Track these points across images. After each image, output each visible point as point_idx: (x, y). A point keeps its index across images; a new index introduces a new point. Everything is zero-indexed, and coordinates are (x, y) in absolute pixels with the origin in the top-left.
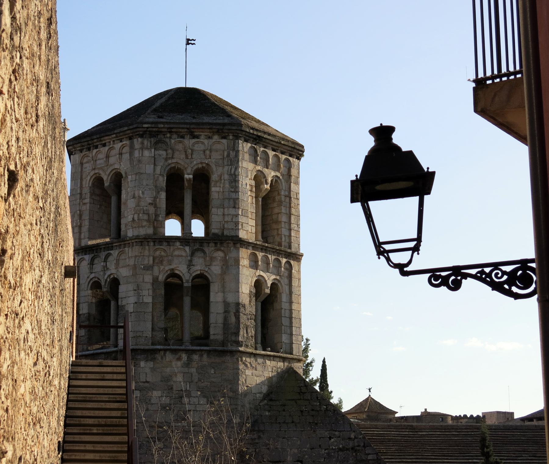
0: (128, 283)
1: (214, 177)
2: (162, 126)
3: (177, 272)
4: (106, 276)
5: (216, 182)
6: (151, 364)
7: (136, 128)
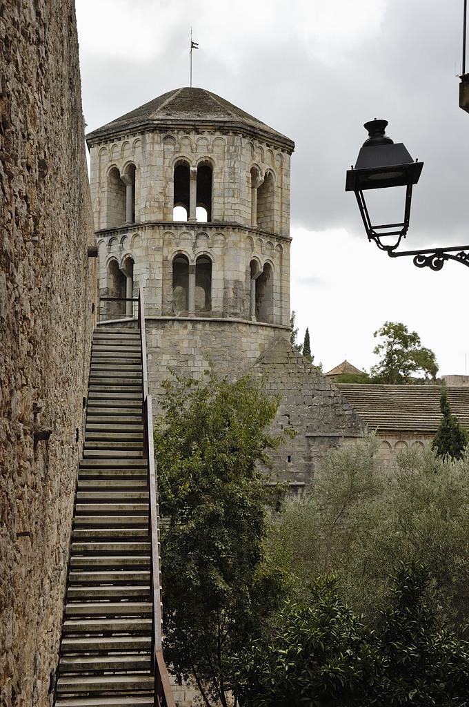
0: (141, 262)
1: (216, 170)
2: (170, 123)
3: (183, 253)
4: (122, 257)
5: (218, 173)
6: (161, 332)
7: (147, 124)
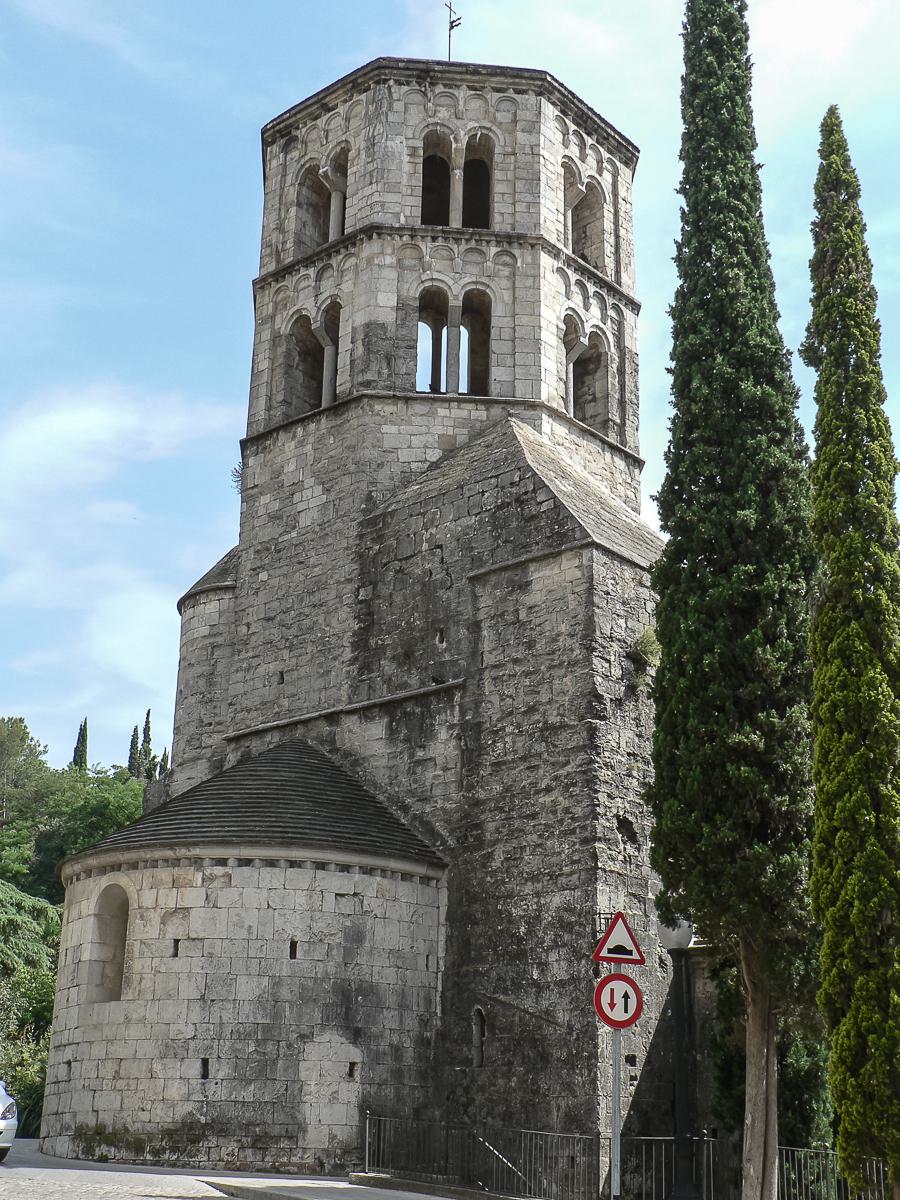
5: (354, 159)
